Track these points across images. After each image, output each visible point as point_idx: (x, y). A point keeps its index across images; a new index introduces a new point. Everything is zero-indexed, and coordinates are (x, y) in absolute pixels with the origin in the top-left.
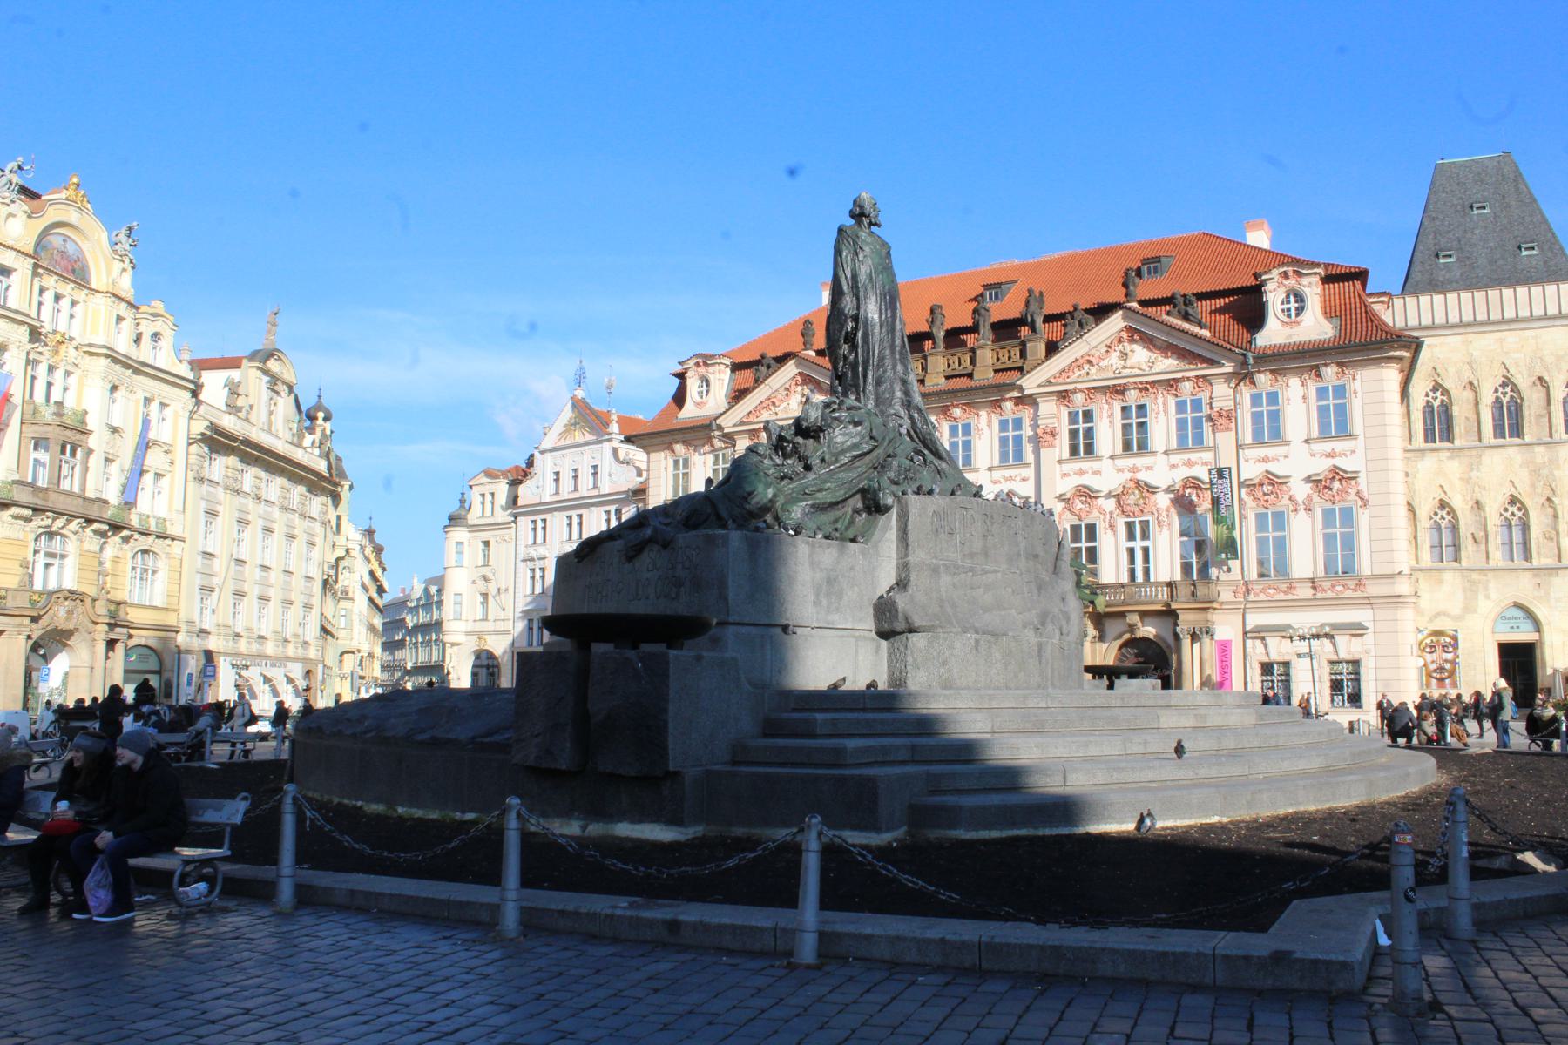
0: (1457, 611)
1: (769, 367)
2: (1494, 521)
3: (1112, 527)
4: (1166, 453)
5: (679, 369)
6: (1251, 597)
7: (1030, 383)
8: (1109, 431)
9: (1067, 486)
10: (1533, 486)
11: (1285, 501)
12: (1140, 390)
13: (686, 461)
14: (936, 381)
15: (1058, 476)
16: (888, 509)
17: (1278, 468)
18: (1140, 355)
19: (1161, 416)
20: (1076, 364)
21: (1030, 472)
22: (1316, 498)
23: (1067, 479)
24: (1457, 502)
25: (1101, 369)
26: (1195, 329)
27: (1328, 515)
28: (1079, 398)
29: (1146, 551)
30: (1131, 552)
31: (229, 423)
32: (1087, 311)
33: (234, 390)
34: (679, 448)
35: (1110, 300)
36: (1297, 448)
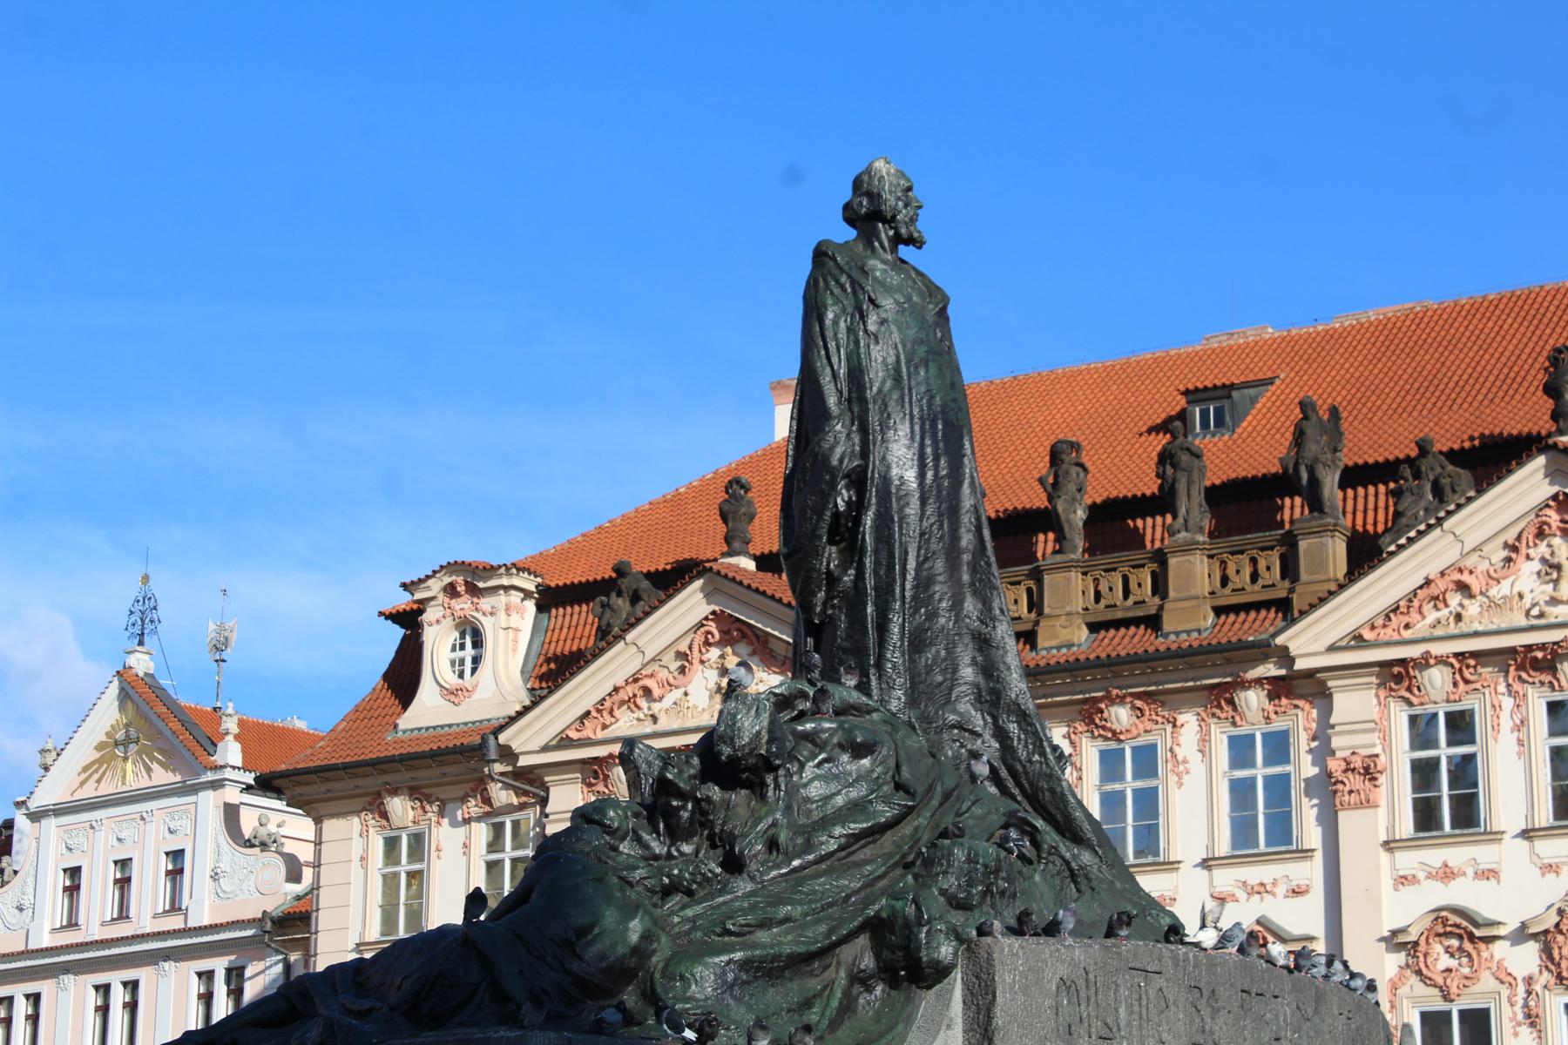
1: (635, 598)
5: (402, 601)
8: (1520, 765)
9: (1408, 909)
13: (418, 841)
14: (1064, 635)
15: (1386, 882)
16: (941, 972)
20: (1427, 593)
21: (1312, 872)
23: (1406, 890)
25: (1493, 605)
28: (1437, 680)
32: (1454, 456)
34: (400, 808)
35: (1513, 424)
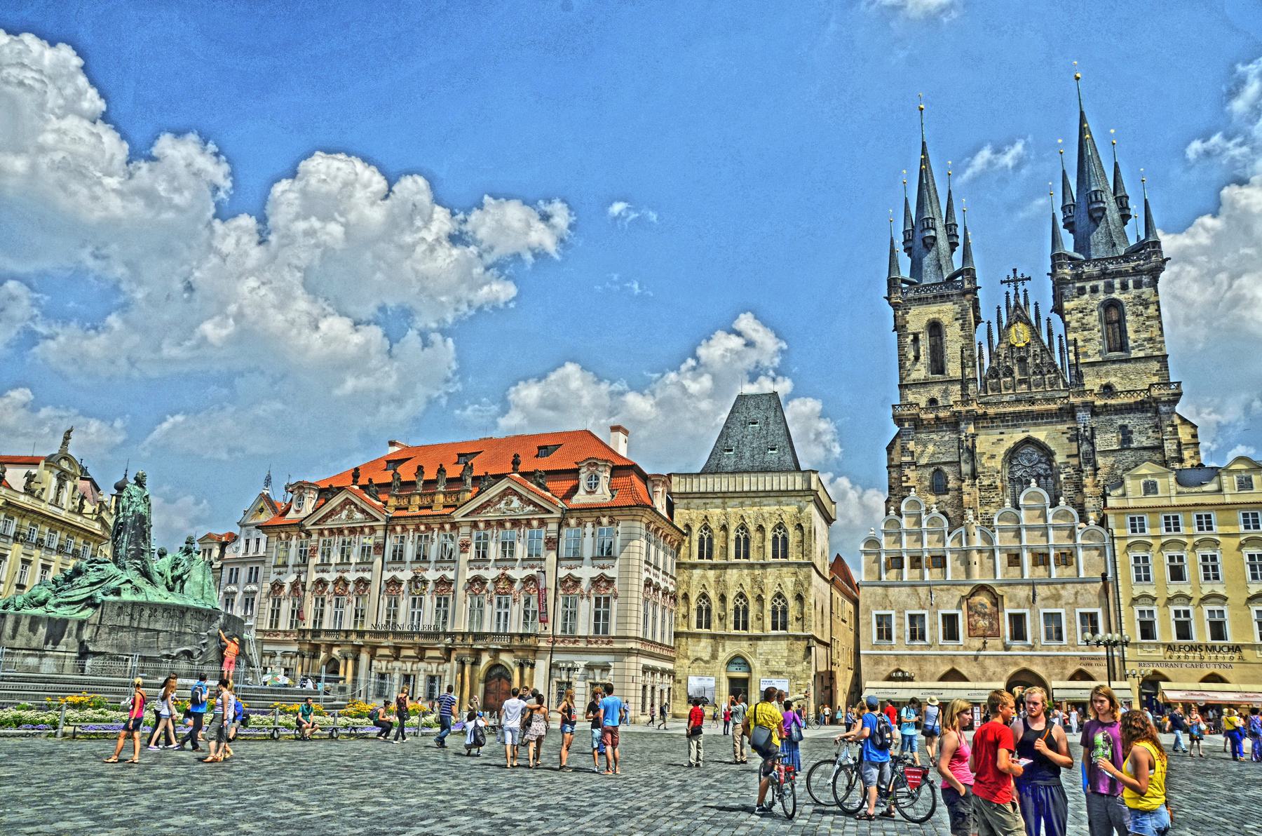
0: (707, 658)
2: (730, 606)
3: (491, 601)
17: (576, 573)
18: (516, 503)
24: (712, 594)
27: (598, 600)
29: (506, 614)
31: (24, 500)
33: (30, 478)
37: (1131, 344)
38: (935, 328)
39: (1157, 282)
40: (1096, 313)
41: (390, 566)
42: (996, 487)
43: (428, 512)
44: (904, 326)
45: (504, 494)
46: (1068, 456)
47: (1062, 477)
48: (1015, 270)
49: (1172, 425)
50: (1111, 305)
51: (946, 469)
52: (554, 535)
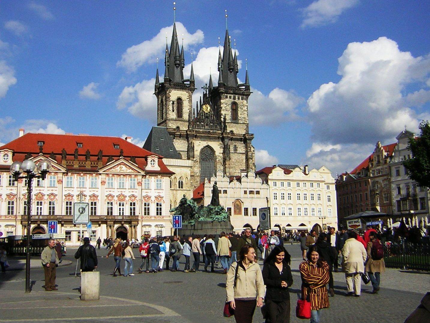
3: (117, 203)
4: (128, 189)
6: (143, 219)
7: (101, 172)
10: (173, 198)
11: (150, 200)
12: (124, 175)
17: (149, 194)
18: (124, 168)
19: (127, 181)
20: (111, 168)
22: (156, 201)
26: (136, 165)
28: (111, 175)
29: (123, 209)
30: (120, 209)
36: (153, 191)
37: (239, 118)
38: (179, 100)
39: (247, 99)
40: (230, 106)
41: (66, 189)
42: (197, 161)
43: (82, 168)
44: (169, 97)
45: (120, 164)
46: (220, 153)
47: (217, 160)
48: (206, 84)
49: (250, 147)
50: (234, 104)
51: (181, 153)
52: (141, 181)
